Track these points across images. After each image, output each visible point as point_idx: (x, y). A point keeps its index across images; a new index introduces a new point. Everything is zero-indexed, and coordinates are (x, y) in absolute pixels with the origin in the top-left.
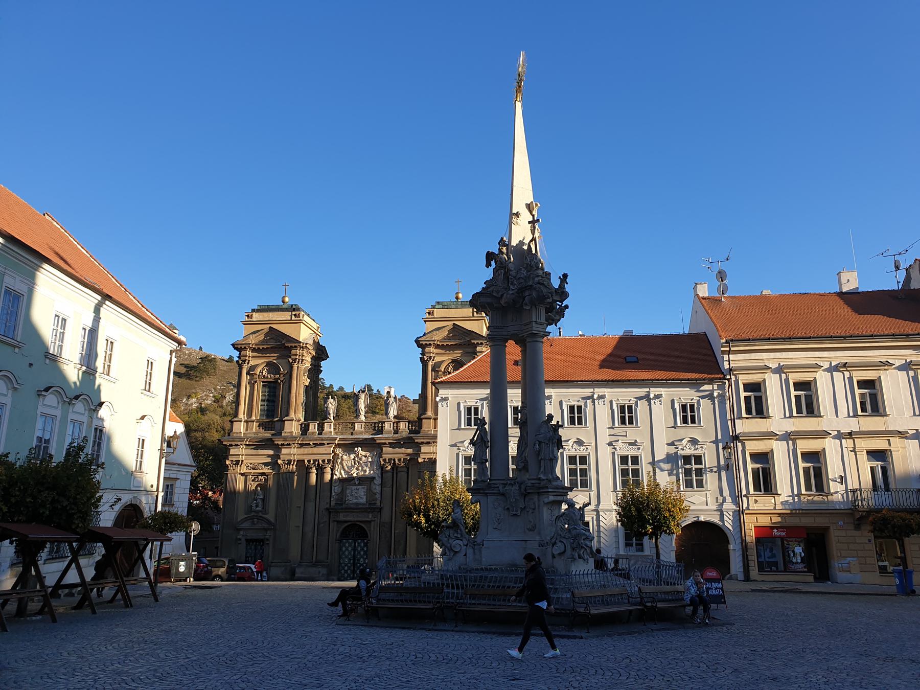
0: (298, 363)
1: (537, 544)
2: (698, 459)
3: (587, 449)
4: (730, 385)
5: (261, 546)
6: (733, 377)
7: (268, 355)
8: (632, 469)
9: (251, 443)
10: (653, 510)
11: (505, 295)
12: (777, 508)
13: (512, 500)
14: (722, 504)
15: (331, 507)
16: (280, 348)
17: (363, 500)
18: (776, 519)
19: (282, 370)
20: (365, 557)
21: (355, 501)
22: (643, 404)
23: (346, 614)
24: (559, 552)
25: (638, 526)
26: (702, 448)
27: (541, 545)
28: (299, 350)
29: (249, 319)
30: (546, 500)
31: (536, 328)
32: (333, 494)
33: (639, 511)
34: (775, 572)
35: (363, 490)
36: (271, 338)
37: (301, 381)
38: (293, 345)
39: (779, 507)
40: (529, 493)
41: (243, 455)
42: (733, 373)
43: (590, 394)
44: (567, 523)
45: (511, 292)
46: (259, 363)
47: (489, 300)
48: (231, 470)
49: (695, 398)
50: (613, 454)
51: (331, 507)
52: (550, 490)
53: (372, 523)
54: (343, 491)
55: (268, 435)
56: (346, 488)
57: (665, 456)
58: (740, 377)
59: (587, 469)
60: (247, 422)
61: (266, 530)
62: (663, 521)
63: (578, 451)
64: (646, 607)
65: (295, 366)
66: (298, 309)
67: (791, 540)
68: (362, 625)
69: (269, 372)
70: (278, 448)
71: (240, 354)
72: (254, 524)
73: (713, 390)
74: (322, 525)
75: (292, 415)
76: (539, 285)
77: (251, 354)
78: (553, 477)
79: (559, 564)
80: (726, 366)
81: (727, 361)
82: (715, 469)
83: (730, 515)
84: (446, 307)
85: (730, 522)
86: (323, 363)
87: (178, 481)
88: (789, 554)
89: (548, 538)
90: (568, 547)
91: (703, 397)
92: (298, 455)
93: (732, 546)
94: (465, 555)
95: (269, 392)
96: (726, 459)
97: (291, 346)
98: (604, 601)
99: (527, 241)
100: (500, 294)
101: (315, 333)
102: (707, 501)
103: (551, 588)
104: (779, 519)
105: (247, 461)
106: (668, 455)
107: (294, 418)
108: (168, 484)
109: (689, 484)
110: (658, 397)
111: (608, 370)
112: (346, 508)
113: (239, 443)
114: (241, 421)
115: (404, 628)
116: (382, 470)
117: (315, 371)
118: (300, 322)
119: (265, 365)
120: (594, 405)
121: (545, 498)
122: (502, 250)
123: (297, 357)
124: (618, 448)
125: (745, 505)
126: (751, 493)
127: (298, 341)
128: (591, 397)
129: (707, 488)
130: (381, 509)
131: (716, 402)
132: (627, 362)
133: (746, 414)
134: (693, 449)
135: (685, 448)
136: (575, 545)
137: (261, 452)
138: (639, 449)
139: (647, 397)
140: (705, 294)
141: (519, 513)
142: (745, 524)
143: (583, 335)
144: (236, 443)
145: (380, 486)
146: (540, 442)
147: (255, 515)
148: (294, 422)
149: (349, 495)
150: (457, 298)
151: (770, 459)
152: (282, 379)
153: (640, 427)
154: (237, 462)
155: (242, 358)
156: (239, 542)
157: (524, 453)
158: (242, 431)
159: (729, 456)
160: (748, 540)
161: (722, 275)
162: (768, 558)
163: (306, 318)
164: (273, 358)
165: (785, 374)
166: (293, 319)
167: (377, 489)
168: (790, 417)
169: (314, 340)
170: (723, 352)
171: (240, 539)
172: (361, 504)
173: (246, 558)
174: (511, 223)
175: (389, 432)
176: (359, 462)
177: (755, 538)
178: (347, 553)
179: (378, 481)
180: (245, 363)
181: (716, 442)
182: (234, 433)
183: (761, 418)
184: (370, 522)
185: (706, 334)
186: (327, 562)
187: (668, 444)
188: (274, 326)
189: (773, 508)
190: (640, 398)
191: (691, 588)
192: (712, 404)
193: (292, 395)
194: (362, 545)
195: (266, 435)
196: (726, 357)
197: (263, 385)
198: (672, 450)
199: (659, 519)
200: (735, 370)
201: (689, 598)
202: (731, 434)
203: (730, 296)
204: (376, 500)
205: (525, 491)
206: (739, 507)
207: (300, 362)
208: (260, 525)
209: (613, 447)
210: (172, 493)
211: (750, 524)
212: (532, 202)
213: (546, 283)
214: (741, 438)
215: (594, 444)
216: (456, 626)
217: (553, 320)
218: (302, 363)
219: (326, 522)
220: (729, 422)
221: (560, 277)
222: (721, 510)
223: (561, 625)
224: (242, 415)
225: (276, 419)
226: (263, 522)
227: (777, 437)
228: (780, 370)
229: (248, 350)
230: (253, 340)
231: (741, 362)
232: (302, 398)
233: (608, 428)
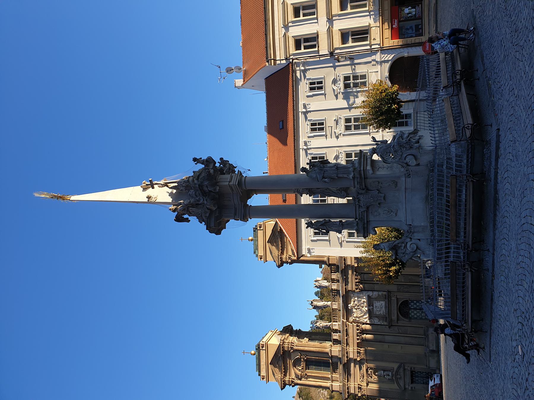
0: (293, 346)
1: (408, 180)
2: (347, 78)
3: (341, 153)
4: (296, 59)
6: (291, 57)
7: (288, 365)
8: (354, 123)
9: (346, 379)
10: (381, 104)
11: (208, 206)
12: (379, 26)
13: (372, 201)
14: (377, 62)
15: (388, 324)
16: (284, 358)
17: (383, 303)
18: (386, 26)
19: (298, 357)
20: (420, 302)
21: (384, 308)
22: (310, 116)
23: (477, 347)
24: (415, 161)
25: (393, 114)
26: (339, 76)
27: (409, 175)
28: (285, 345)
29: (265, 378)
30: (371, 172)
31: (234, 182)
32: (379, 323)
33: (382, 114)
34: (422, 21)
35: (376, 303)
36: (278, 363)
37: (306, 344)
38: (282, 349)
39: (378, 24)
40: (365, 187)
41: (355, 384)
42: (288, 57)
43: (304, 151)
44: (389, 154)
45: (205, 202)
46: (293, 372)
47: (213, 219)
48: (365, 393)
49: (305, 82)
50: (344, 135)
51: (388, 324)
52: (362, 169)
53: (398, 297)
54: (377, 317)
55: (341, 367)
56: (375, 314)
57: (345, 100)
58: (291, 52)
59: (355, 153)
60: (332, 381)
61: (404, 369)
62: (389, 97)
63: (342, 159)
64: (461, 79)
65: (295, 348)
66: (259, 345)
67: (400, 16)
68: (490, 339)
69: (300, 365)
70: (350, 360)
71: (288, 385)
73: (300, 70)
74: (400, 330)
75: (327, 350)
76: (199, 179)
77: (288, 377)
78: (352, 166)
79: (425, 159)
80: (284, 62)
81: (280, 62)
82: (353, 67)
83: (384, 56)
84: (257, 248)
85: (389, 56)
86: (294, 329)
88: (410, 17)
89: (403, 170)
90: (409, 152)
91: (305, 77)
92: (354, 347)
93: (405, 54)
94: (419, 240)
95: (313, 365)
96: (346, 59)
97: (282, 350)
98: (458, 116)
99: (170, 191)
100: (207, 210)
101: (274, 334)
102: (375, 72)
103: (447, 166)
104: (386, 24)
105: (359, 381)
106: (344, 99)
107: (329, 349)
109: (364, 84)
110: (305, 106)
111: (288, 140)
112: (389, 315)
113: (347, 387)
114: (332, 385)
115: (492, 300)
116: (363, 290)
117: (300, 334)
118: (267, 344)
119: (295, 368)
120: (311, 148)
121: (369, 172)
122: (173, 209)
123: (290, 346)
124: (340, 132)
125: (377, 46)
126: (369, 43)
127: (279, 346)
128: (306, 150)
129: (366, 72)
130: (389, 292)
131: (308, 68)
132: (283, 128)
133: (316, 48)
134: (339, 82)
135: (339, 87)
136: (408, 146)
137: (352, 372)
138: (340, 118)
139: (305, 113)
140: (241, 81)
141: (382, 195)
142: (390, 46)
143: (267, 158)
144: (346, 389)
145: (374, 292)
146: (324, 178)
148: (332, 349)
149: (380, 313)
150: (252, 240)
151: (345, 31)
152: (304, 357)
153: (325, 118)
154: (360, 388)
155: (291, 383)
156: (413, 389)
157: (333, 191)
158: (338, 384)
159: (344, 58)
160: (400, 43)
161: (229, 70)
162: (413, 30)
163: (264, 340)
164: (290, 362)
165: (289, 24)
166: (265, 349)
167: (376, 294)
168: (317, 19)
169: (279, 335)
170: (275, 64)
171: (412, 388)
172: (386, 305)
173: (424, 384)
174: (155, 203)
175: (338, 286)
176: (358, 306)
177: (399, 39)
178: (418, 314)
179: (370, 293)
180: (294, 382)
181: (335, 67)
182: (340, 390)
183: (318, 38)
184: (397, 299)
185: (266, 78)
186: (425, 327)
187: (337, 98)
189: (379, 28)
190: (306, 118)
191: (442, 44)
192: (309, 70)
193: (315, 350)
194: (412, 304)
195: (341, 368)
196: (278, 62)
197: (308, 369)
198: (341, 96)
199: (387, 99)
200: (287, 56)
201: (452, 46)
202: (329, 57)
203: (243, 65)
204: (382, 294)
205: (363, 189)
206: (379, 50)
207: (293, 344)
208: (402, 373)
209: (339, 136)
211: (389, 43)
212: (141, 186)
213: (198, 174)
214: (332, 51)
215: (338, 148)
216: (488, 250)
217: (230, 169)
218: (294, 343)
219: (398, 328)
220: (321, 59)
221: (195, 164)
222: (381, 62)
223: (483, 152)
224: (328, 384)
225: (330, 361)
226: (399, 371)
227: (331, 27)
228: (286, 27)
229: (285, 379)
230: (279, 376)
231: (281, 52)
232: (316, 343)
233: (326, 139)
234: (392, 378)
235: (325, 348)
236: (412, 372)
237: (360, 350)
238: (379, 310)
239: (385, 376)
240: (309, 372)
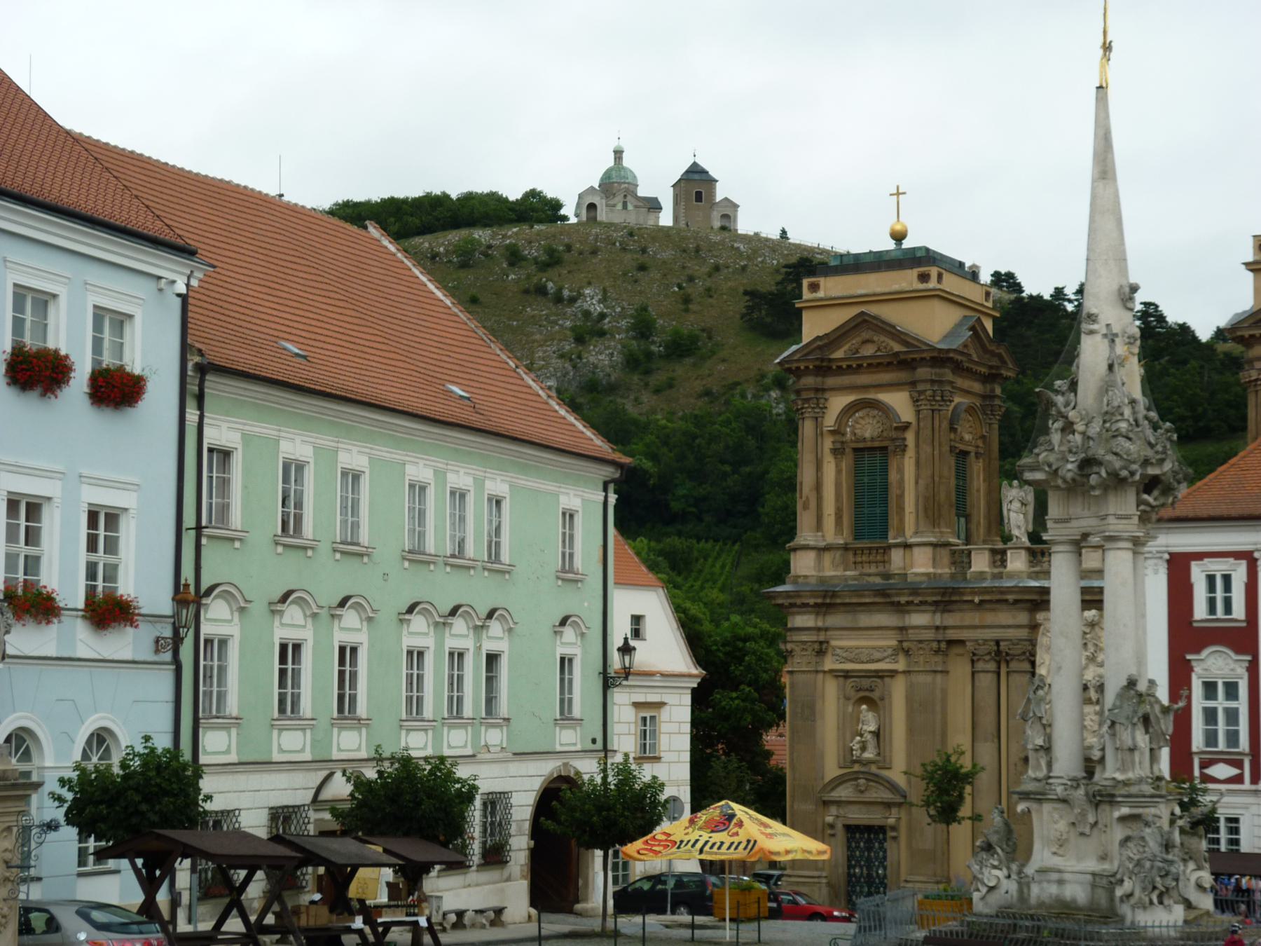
5: (881, 843)
48: (799, 662)
61: (888, 805)
72: (862, 792)
97: (914, 360)
108: (644, 715)
141: (1087, 830)
144: (806, 601)
147: (863, 769)
156: (829, 832)
171: (832, 826)
173: (849, 867)
188: (873, 310)
208: (875, 795)
210: (654, 732)
226: (881, 787)
234: (855, 762)
236: (882, 829)
238: (1086, 723)
239: (858, 738)
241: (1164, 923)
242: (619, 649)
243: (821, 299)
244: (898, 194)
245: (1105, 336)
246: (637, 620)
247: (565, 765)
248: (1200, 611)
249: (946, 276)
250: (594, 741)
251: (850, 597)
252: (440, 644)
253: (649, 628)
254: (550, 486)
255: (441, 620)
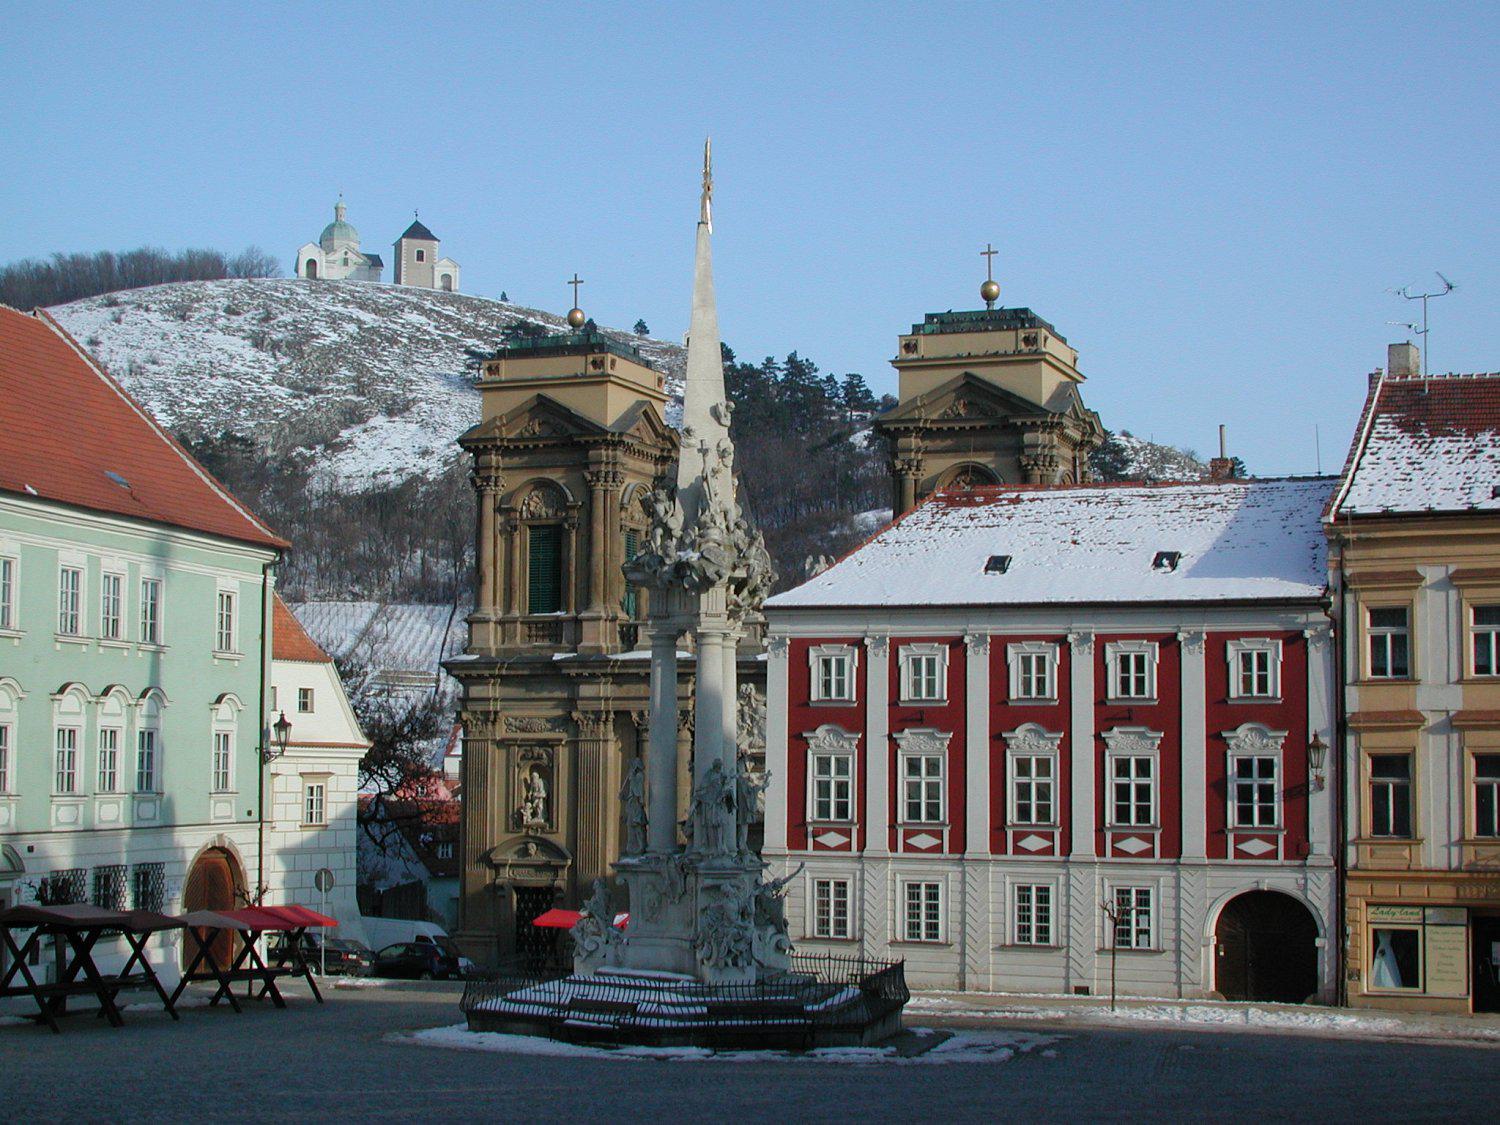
19: (571, 499)
41: (496, 700)
60: (501, 623)
65: (599, 488)
77: (503, 462)
87: (331, 779)
92: (615, 699)
97: (587, 442)
105: (506, 713)
118: (602, 380)
123: (603, 468)
144: (480, 672)
148: (602, 622)
155: (483, 473)
156: (499, 893)
173: (518, 927)
176: (752, 719)
188: (550, 393)
207: (610, 479)
218: (614, 481)
235: (605, 597)
237: (607, 719)
240: (523, 539)
241: (739, 983)
242: (275, 726)
243: (501, 382)
244: (576, 282)
245: (699, 450)
246: (305, 693)
247: (220, 836)
248: (816, 693)
249: (619, 361)
250: (250, 813)
251: (523, 669)
252: (92, 723)
253: (318, 700)
254: (206, 570)
255: (94, 699)
